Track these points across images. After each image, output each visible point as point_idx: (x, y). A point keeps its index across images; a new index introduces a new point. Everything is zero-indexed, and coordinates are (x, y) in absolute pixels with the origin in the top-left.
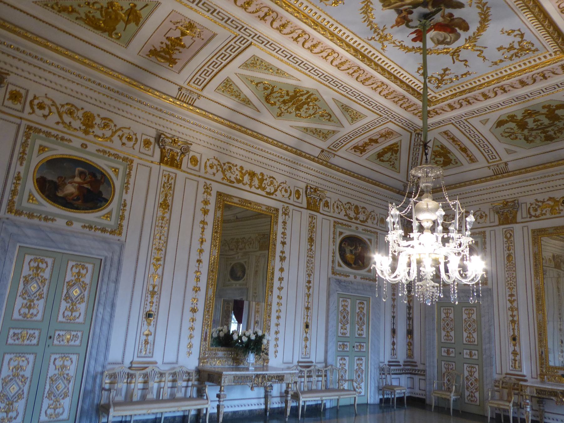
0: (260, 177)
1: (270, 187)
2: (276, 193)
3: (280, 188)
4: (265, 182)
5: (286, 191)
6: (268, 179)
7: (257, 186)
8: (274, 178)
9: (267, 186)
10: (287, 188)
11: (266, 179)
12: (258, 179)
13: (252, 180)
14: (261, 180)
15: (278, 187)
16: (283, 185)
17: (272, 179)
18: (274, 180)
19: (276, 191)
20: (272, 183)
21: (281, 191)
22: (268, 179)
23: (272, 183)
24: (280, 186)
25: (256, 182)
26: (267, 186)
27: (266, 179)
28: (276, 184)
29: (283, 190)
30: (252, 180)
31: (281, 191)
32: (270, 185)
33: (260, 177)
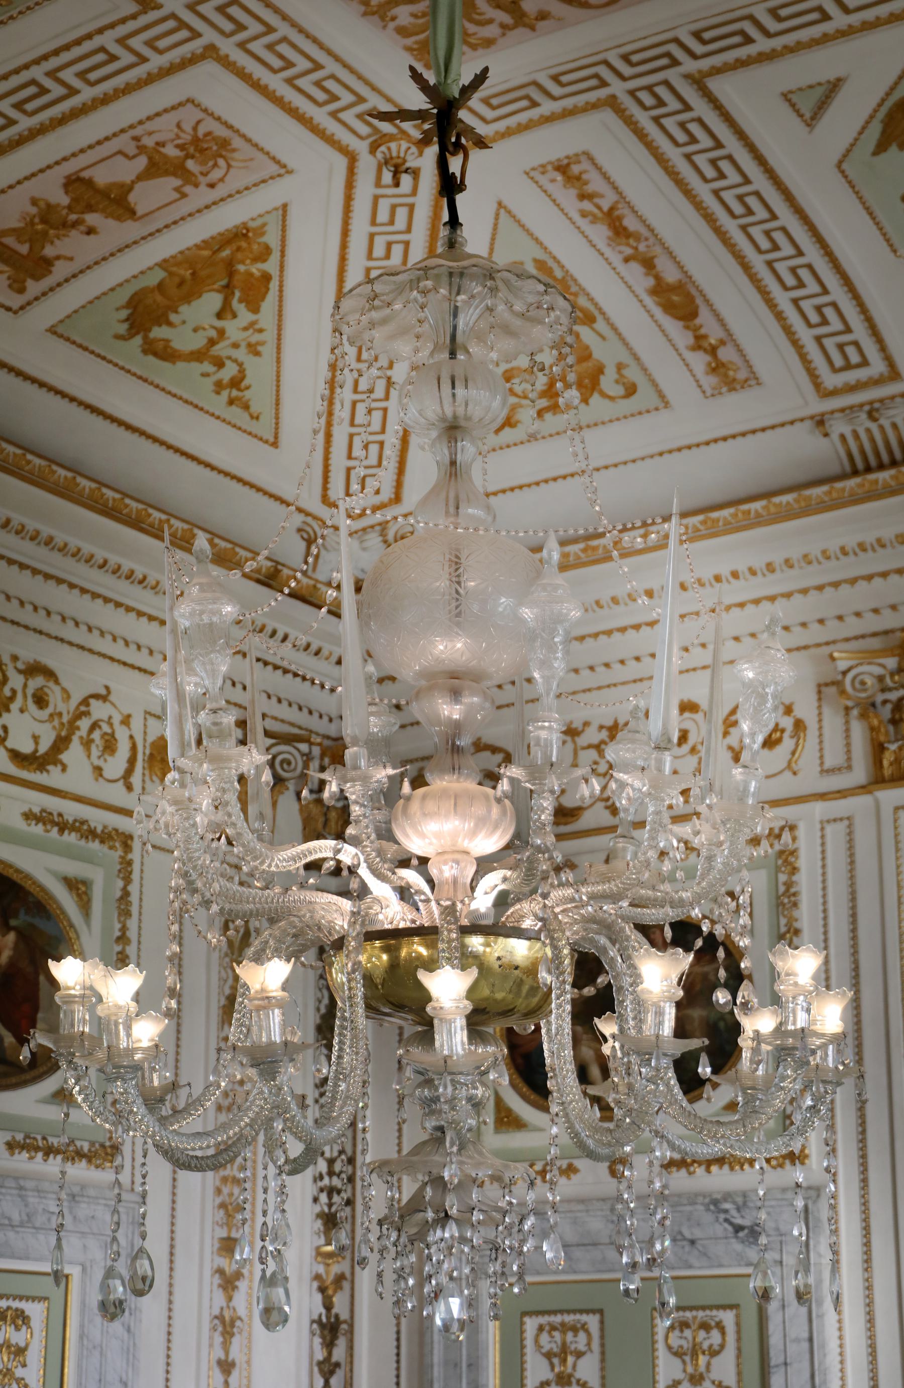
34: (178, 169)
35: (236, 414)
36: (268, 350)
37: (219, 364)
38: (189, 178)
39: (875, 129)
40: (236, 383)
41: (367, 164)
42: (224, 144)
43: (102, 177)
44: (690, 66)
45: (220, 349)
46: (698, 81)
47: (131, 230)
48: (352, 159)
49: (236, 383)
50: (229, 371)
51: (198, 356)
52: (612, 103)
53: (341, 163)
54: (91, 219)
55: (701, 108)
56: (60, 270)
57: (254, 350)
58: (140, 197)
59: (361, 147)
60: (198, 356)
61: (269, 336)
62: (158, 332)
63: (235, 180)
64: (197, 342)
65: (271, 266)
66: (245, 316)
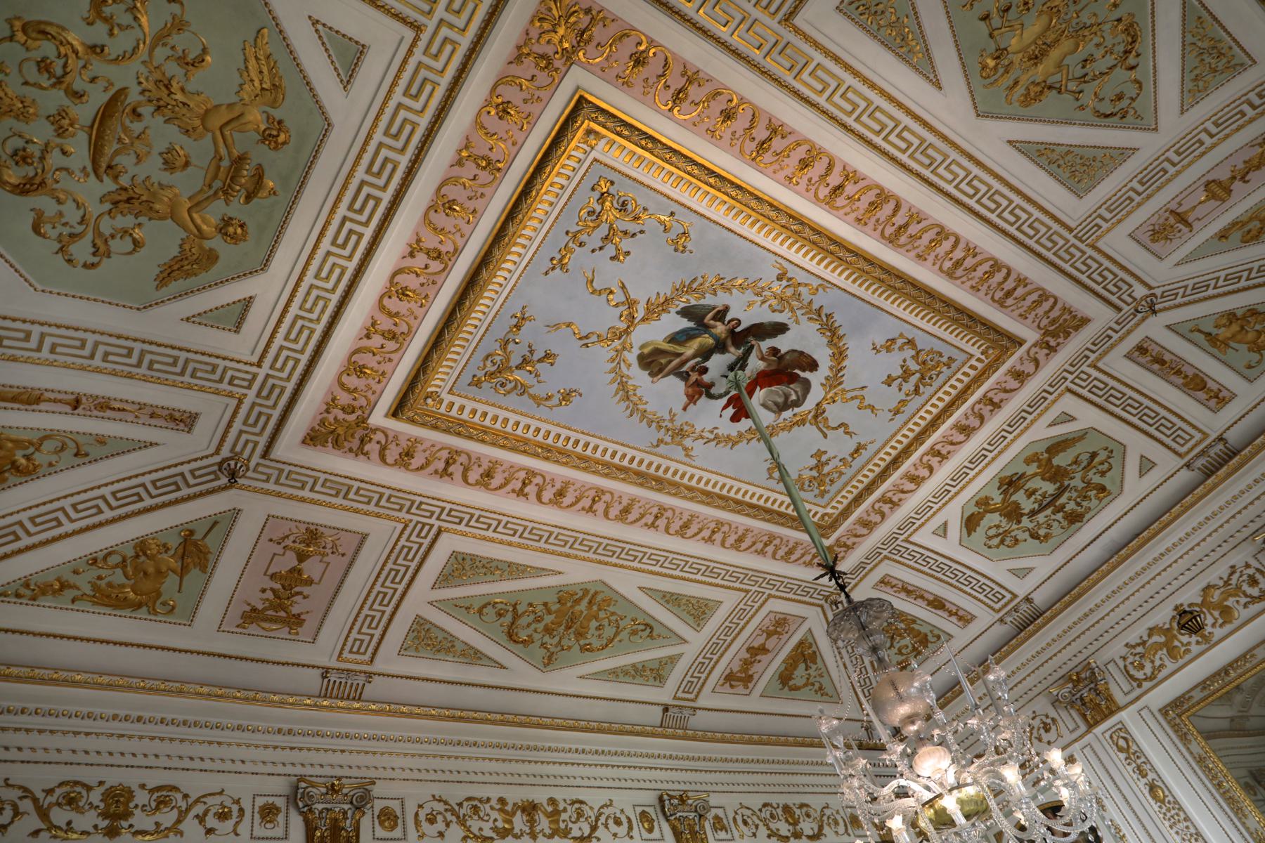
0: (550, 809)
1: (579, 824)
2: (597, 834)
3: (602, 819)
4: (564, 816)
5: (618, 822)
6: (569, 808)
7: (548, 831)
8: (582, 802)
9: (570, 825)
10: (618, 815)
11: (565, 810)
12: (549, 815)
13: (532, 822)
14: (554, 815)
15: (597, 819)
16: (607, 811)
17: (577, 806)
18: (583, 806)
19: (594, 828)
20: (580, 814)
21: (606, 826)
22: (569, 808)
23: (580, 814)
24: (601, 814)
25: (544, 824)
26: (570, 825)
27: (565, 810)
28: (590, 813)
29: (611, 822)
30: (532, 822)
31: (606, 826)
32: (578, 819)
33: (550, 809)
34: (776, 632)
35: (825, 698)
36: (825, 674)
37: (813, 684)
38: (779, 633)
39: (964, 530)
40: (821, 688)
41: (826, 606)
42: (785, 619)
43: (756, 644)
44: (902, 538)
45: (812, 680)
46: (907, 541)
47: (770, 656)
48: (822, 607)
49: (821, 688)
50: (817, 685)
51: (806, 685)
52: (886, 557)
53: (819, 609)
54: (758, 658)
55: (911, 547)
56: (756, 677)
57: (821, 676)
58: (769, 645)
59: (823, 602)
60: (806, 685)
61: (823, 670)
62: (791, 683)
63: (793, 628)
64: (804, 680)
65: (814, 648)
66: (814, 667)
